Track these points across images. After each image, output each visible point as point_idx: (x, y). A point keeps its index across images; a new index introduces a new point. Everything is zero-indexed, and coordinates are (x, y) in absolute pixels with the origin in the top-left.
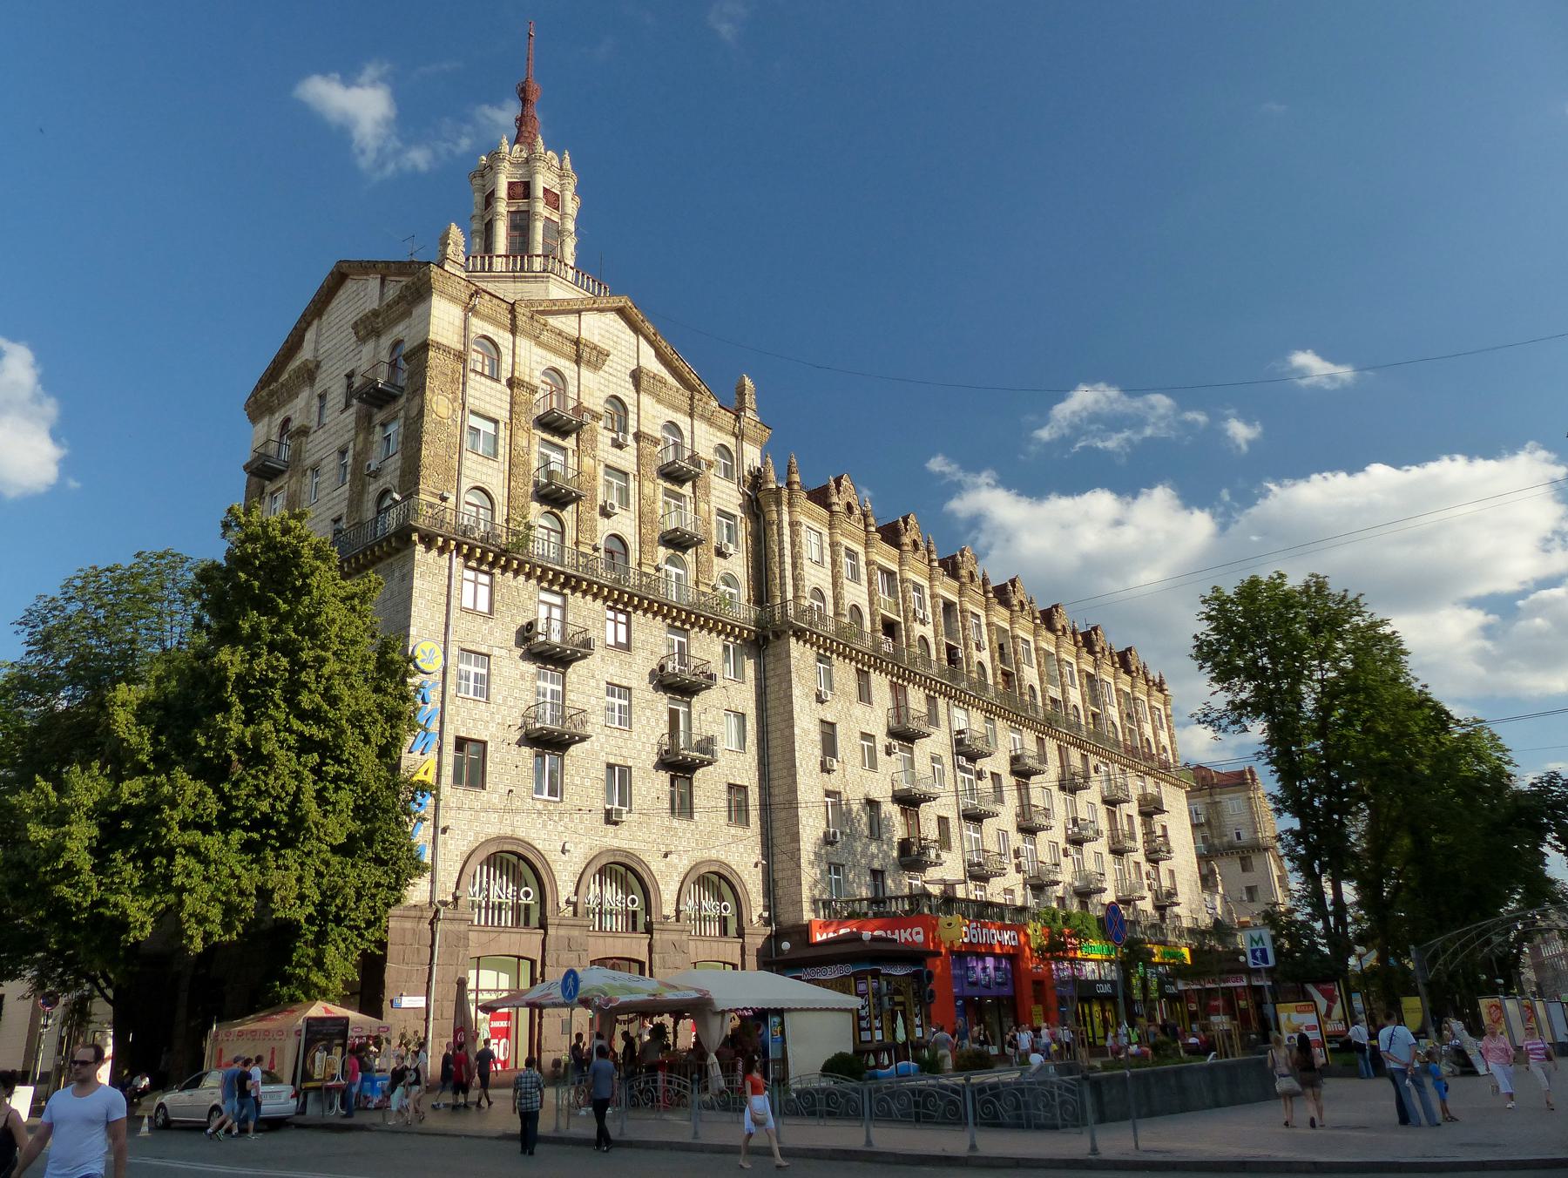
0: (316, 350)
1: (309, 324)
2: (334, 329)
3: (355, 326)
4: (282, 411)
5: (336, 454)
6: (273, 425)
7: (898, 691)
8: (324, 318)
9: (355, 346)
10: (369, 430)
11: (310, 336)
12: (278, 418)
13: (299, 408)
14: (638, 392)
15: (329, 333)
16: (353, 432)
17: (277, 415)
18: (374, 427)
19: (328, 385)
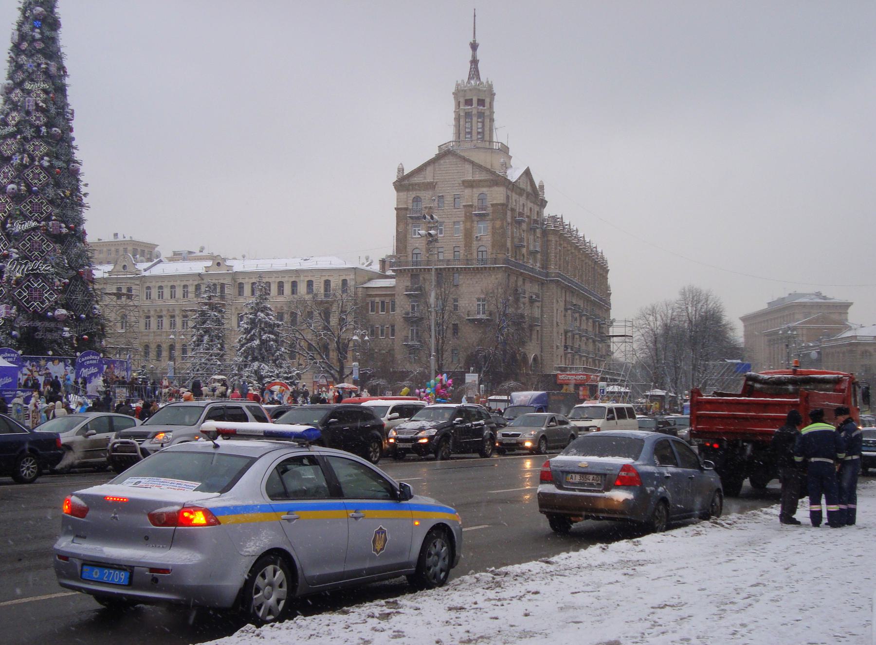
0: (434, 176)
1: (429, 165)
2: (444, 172)
3: (464, 182)
4: (414, 192)
5: (453, 224)
6: (409, 196)
7: (565, 292)
8: (437, 164)
9: (458, 185)
10: (472, 221)
11: (430, 169)
12: (413, 194)
13: (426, 195)
14: (527, 200)
15: (440, 172)
16: (463, 219)
17: (411, 193)
18: (473, 221)
19: (446, 194)
